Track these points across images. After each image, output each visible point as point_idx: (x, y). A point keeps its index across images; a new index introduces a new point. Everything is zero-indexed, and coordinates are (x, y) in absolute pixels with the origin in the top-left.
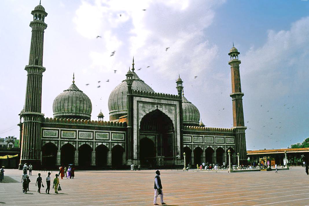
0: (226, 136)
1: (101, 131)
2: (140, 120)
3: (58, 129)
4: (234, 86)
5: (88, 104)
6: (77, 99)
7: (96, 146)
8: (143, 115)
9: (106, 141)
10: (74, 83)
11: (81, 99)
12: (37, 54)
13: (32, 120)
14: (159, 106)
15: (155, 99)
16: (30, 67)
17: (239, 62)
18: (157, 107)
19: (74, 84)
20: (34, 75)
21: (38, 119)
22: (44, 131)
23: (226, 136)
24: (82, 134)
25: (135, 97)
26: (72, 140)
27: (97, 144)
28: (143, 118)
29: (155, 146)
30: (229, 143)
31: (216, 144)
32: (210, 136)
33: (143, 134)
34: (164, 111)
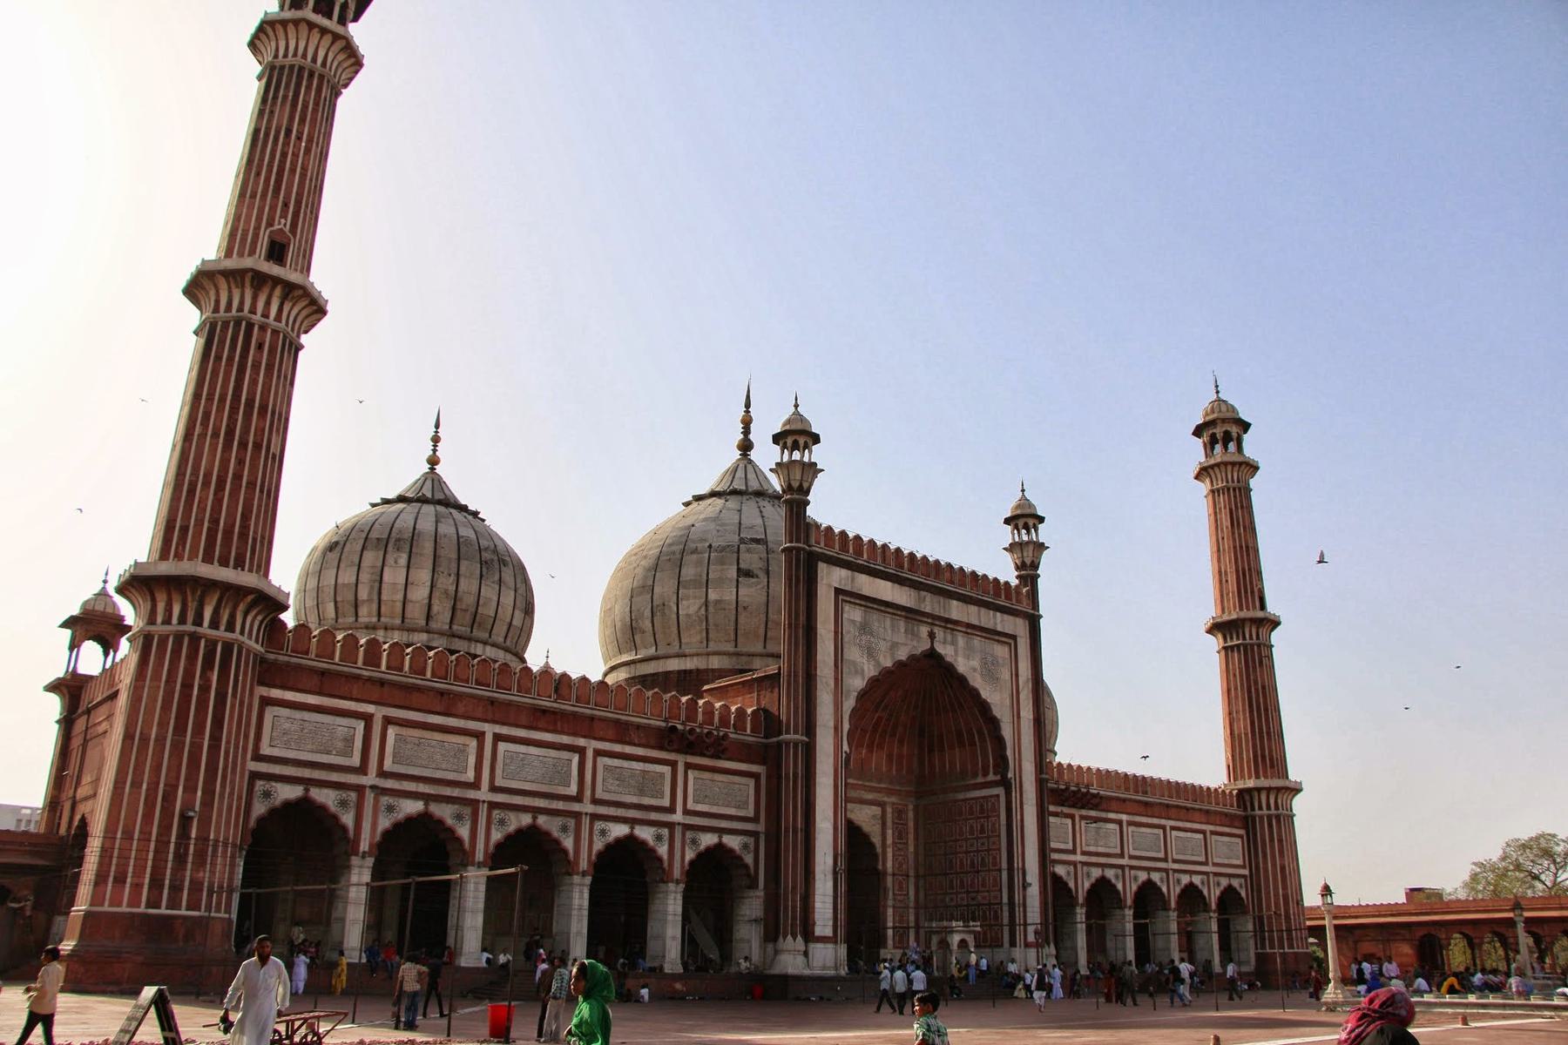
1: (628, 749)
2: (849, 704)
3: (370, 709)
4: (1232, 578)
6: (463, 549)
7: (599, 845)
8: (863, 679)
9: (654, 816)
10: (432, 469)
11: (486, 556)
12: (286, 205)
13: (200, 625)
15: (923, 593)
16: (229, 274)
17: (1241, 464)
18: (932, 635)
20: (250, 326)
22: (270, 712)
24: (511, 756)
25: (825, 565)
27: (603, 833)
29: (880, 867)
30: (1226, 861)
31: (1176, 866)
34: (962, 666)
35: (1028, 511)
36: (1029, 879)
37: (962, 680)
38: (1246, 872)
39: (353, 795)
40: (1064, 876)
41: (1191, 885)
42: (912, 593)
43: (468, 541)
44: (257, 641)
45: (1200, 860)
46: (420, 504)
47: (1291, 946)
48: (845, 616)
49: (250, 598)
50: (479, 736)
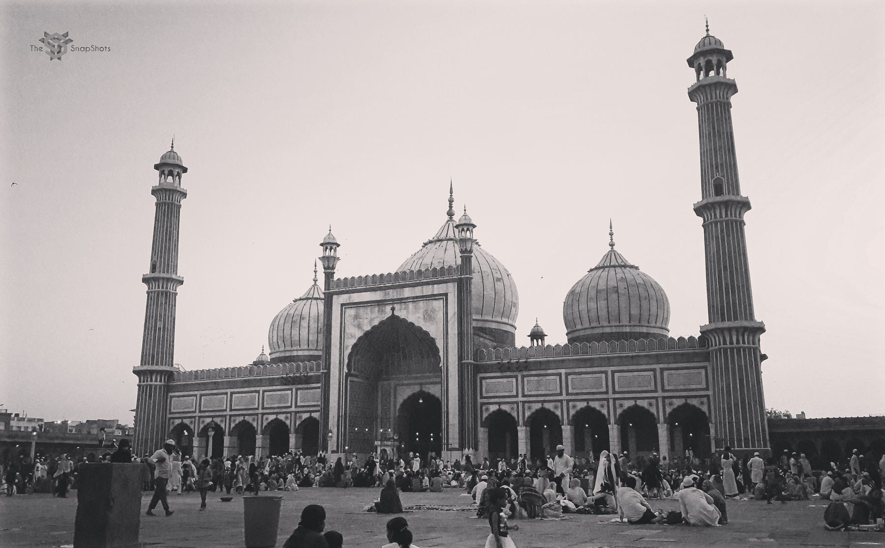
0: (665, 366)
1: (274, 388)
2: (348, 352)
3: (196, 393)
5: (313, 325)
7: (265, 424)
8: (355, 339)
9: (284, 410)
10: (315, 283)
14: (397, 306)
18: (393, 309)
19: (315, 284)
21: (154, 379)
23: (665, 366)
26: (221, 413)
28: (355, 346)
31: (617, 396)
32: (589, 370)
33: (411, 381)
34: (411, 319)
35: (467, 222)
36: (450, 416)
37: (412, 324)
38: (710, 393)
39: (193, 419)
40: (509, 411)
41: (636, 406)
42: (382, 293)
43: (290, 314)
44: (161, 381)
45: (649, 388)
46: (306, 301)
47: (747, 445)
48: (347, 314)
49: (148, 372)
50: (226, 394)
